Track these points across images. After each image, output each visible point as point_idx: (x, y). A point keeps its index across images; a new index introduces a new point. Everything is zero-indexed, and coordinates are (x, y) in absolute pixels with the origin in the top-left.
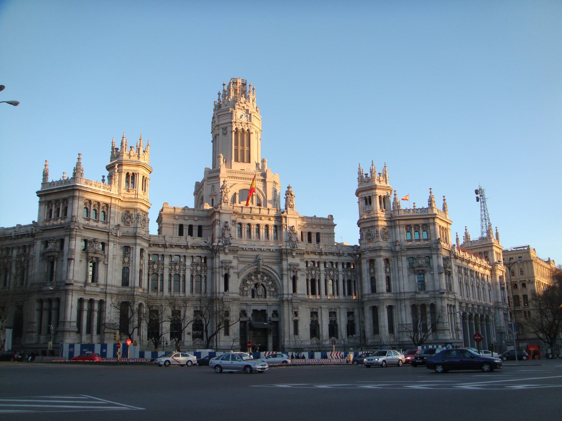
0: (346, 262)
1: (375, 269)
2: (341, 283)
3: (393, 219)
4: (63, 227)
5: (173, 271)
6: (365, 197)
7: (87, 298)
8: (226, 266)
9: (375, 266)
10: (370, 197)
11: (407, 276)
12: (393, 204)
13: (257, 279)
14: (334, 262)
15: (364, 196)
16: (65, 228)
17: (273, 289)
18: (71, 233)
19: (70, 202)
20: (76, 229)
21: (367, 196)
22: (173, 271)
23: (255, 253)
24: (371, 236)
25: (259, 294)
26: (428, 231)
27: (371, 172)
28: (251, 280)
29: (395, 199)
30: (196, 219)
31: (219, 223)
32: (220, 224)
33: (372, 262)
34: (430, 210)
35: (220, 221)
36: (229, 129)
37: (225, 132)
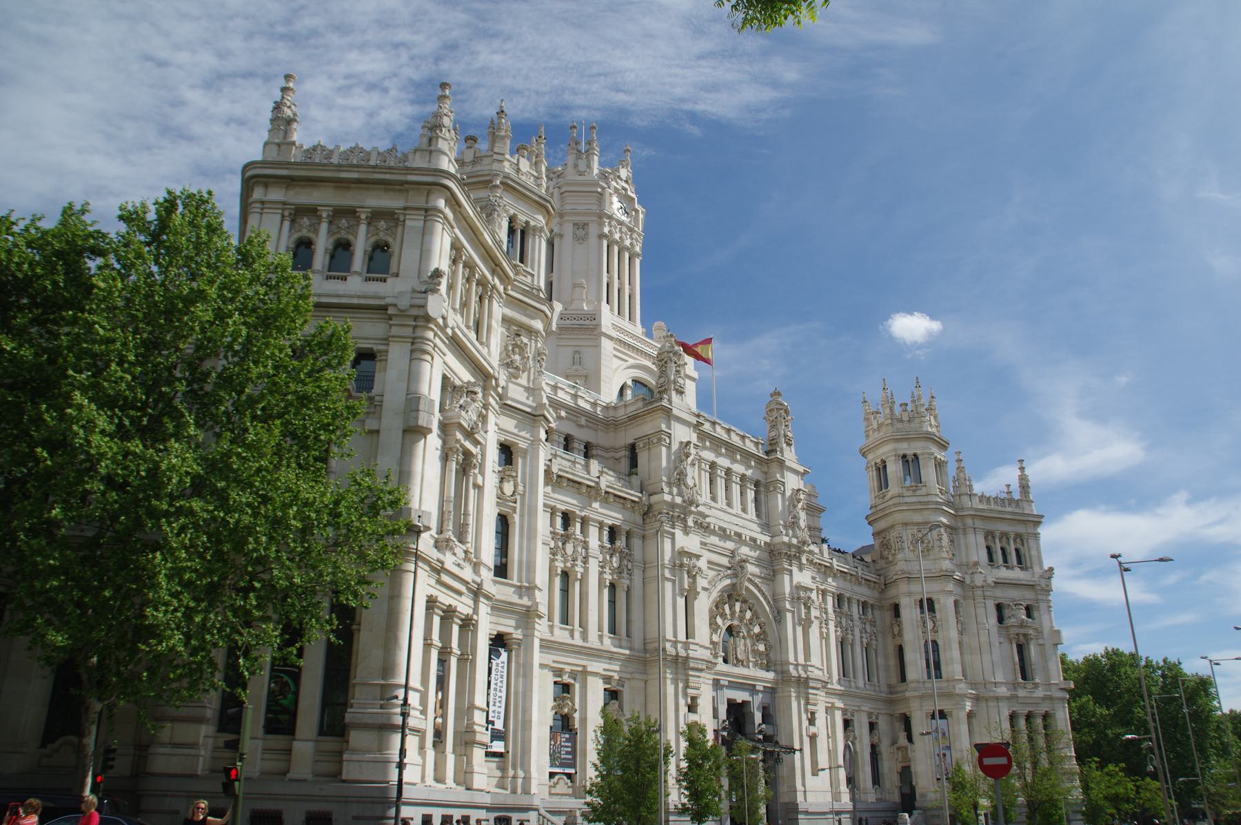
0: (863, 600)
1: (938, 623)
2: (858, 649)
3: (965, 513)
4: (384, 308)
5: (559, 557)
6: (904, 456)
7: (445, 599)
8: (683, 563)
9: (938, 614)
10: (915, 455)
11: (997, 644)
12: (954, 482)
13: (733, 614)
14: (848, 595)
15: (901, 453)
16: (391, 311)
17: (761, 647)
18: (418, 334)
19: (414, 222)
20: (437, 325)
21: (910, 452)
22: (559, 557)
23: (730, 545)
24: (925, 545)
25: (739, 657)
26: (1022, 550)
27: (913, 401)
28: (723, 616)
29: (960, 469)
30: (583, 421)
31: (668, 441)
32: (670, 444)
33: (929, 605)
34: (1025, 505)
35: (670, 436)
36: (593, 230)
37: (581, 233)
